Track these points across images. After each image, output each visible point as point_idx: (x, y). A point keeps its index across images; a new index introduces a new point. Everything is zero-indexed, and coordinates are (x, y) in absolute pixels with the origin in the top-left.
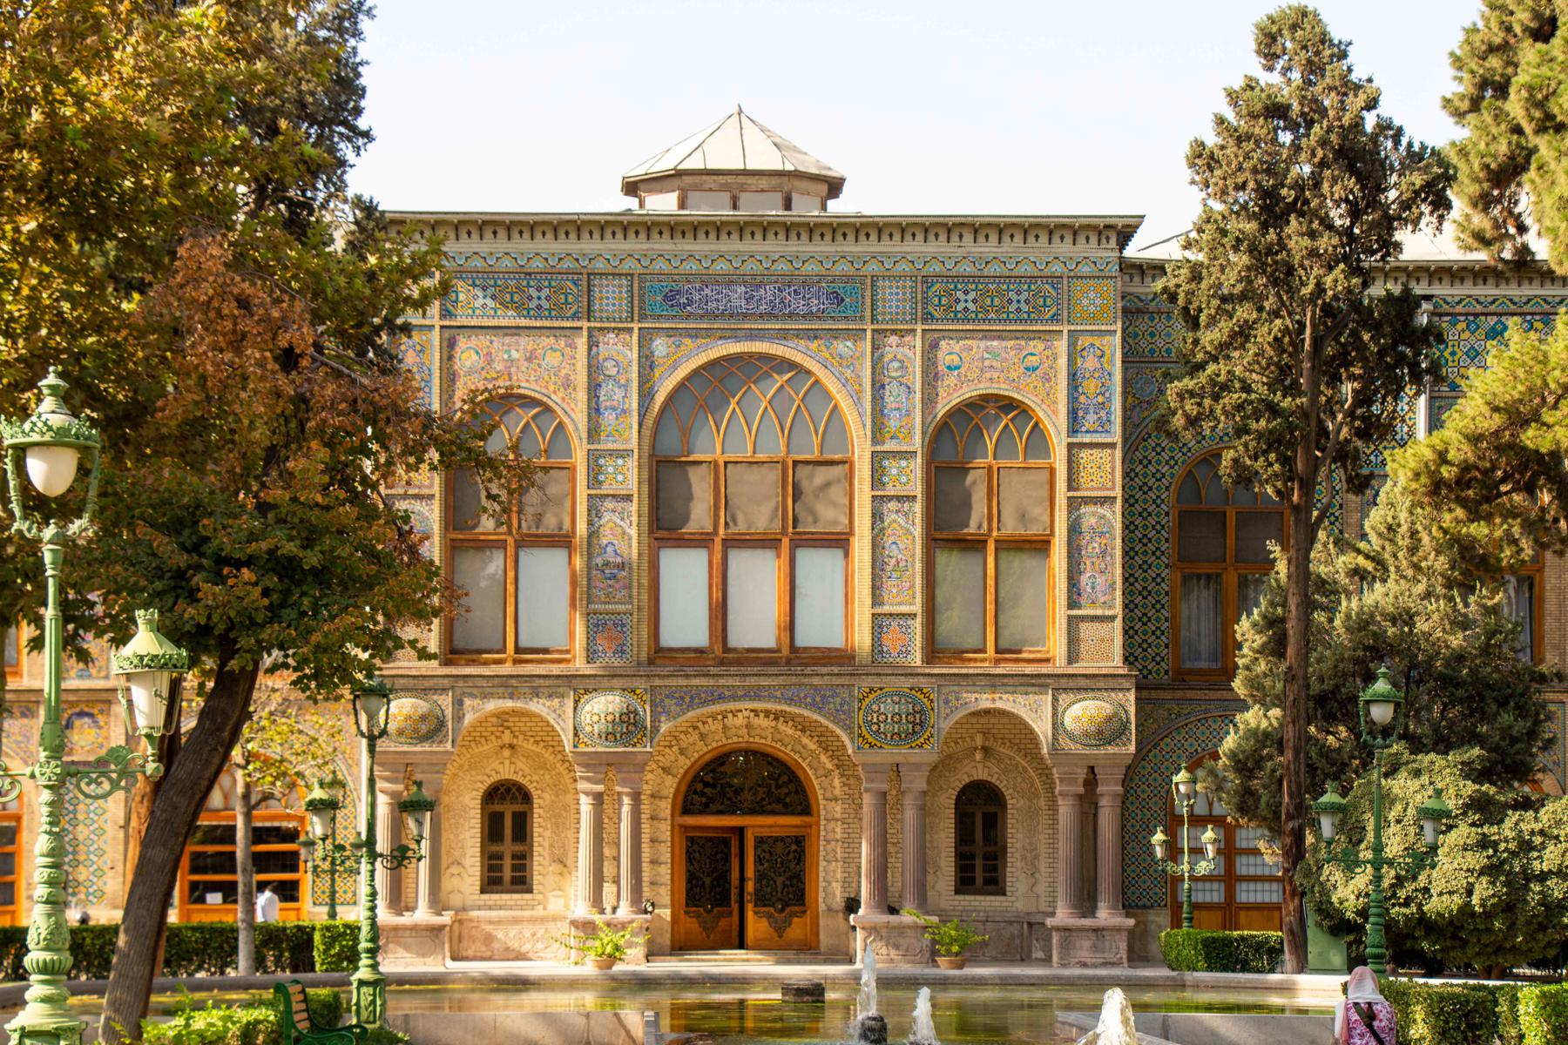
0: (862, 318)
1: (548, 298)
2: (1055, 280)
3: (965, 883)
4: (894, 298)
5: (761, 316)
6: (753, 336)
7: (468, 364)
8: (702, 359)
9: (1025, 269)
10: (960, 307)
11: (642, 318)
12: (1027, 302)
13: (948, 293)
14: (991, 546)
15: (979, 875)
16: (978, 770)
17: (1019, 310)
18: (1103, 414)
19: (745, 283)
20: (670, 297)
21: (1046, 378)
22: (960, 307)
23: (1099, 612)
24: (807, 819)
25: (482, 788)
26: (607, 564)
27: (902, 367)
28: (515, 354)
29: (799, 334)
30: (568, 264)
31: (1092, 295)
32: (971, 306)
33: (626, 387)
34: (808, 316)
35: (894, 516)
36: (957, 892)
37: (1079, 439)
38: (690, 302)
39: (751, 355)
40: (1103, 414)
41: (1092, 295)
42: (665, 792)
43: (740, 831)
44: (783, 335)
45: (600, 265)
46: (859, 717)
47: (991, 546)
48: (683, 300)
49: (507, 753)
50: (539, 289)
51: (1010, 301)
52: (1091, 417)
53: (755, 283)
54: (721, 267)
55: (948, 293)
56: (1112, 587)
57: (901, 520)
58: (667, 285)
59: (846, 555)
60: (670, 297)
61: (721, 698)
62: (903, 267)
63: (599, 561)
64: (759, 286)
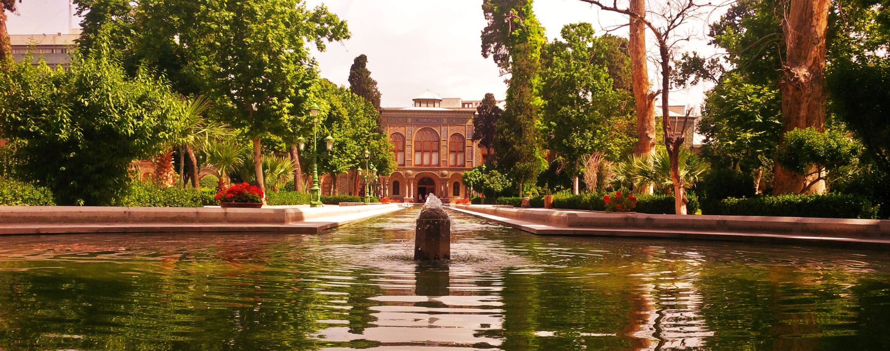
4: (445, 121)
16: (456, 180)
53: (428, 118)
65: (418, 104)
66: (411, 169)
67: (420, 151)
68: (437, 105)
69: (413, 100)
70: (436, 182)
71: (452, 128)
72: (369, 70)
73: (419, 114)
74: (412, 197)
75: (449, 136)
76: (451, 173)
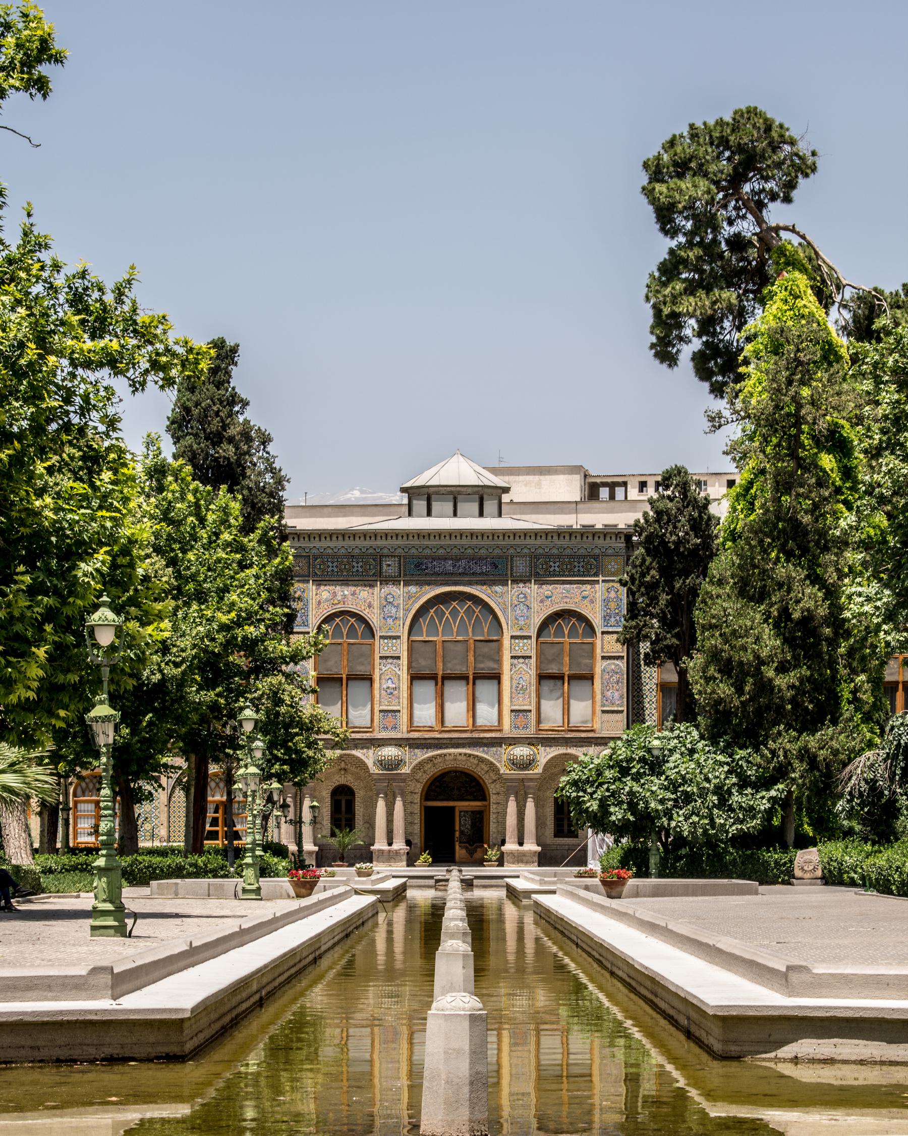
0: (506, 574)
1: (361, 567)
2: (596, 557)
3: (558, 833)
5: (460, 574)
6: (456, 584)
7: (325, 597)
8: (432, 594)
9: (582, 552)
10: (552, 569)
11: (405, 575)
12: (583, 567)
13: (546, 563)
14: (566, 679)
15: (566, 828)
17: (579, 570)
18: (618, 618)
19: (452, 559)
20: (417, 566)
21: (592, 602)
22: (552, 569)
23: (616, 709)
24: (484, 803)
25: (331, 788)
26: (388, 688)
27: (525, 597)
28: (346, 593)
29: (478, 583)
30: (371, 551)
31: (613, 563)
32: (557, 569)
33: (397, 607)
34: (482, 574)
35: (521, 665)
36: (555, 836)
37: (606, 629)
38: (427, 568)
39: (455, 592)
40: (618, 618)
41: (613, 563)
42: (417, 791)
43: (453, 808)
44: (470, 583)
45: (385, 551)
46: (505, 757)
47: (566, 679)
48: (424, 567)
49: (343, 772)
50: (357, 563)
51: (575, 567)
52: (613, 620)
53: (457, 559)
54: (442, 551)
55: (546, 563)
56: (621, 697)
57: (524, 667)
58: (416, 561)
59: (499, 683)
60: (417, 566)
61: (441, 748)
62: (526, 551)
63: (385, 686)
64: (460, 559)
65: (420, 505)
66: (398, 743)
67: (433, 677)
68: (490, 506)
69: (403, 490)
70: (492, 788)
71: (547, 589)
72: (242, 393)
73: (426, 542)
74: (399, 845)
75: (537, 621)
76: (545, 755)
